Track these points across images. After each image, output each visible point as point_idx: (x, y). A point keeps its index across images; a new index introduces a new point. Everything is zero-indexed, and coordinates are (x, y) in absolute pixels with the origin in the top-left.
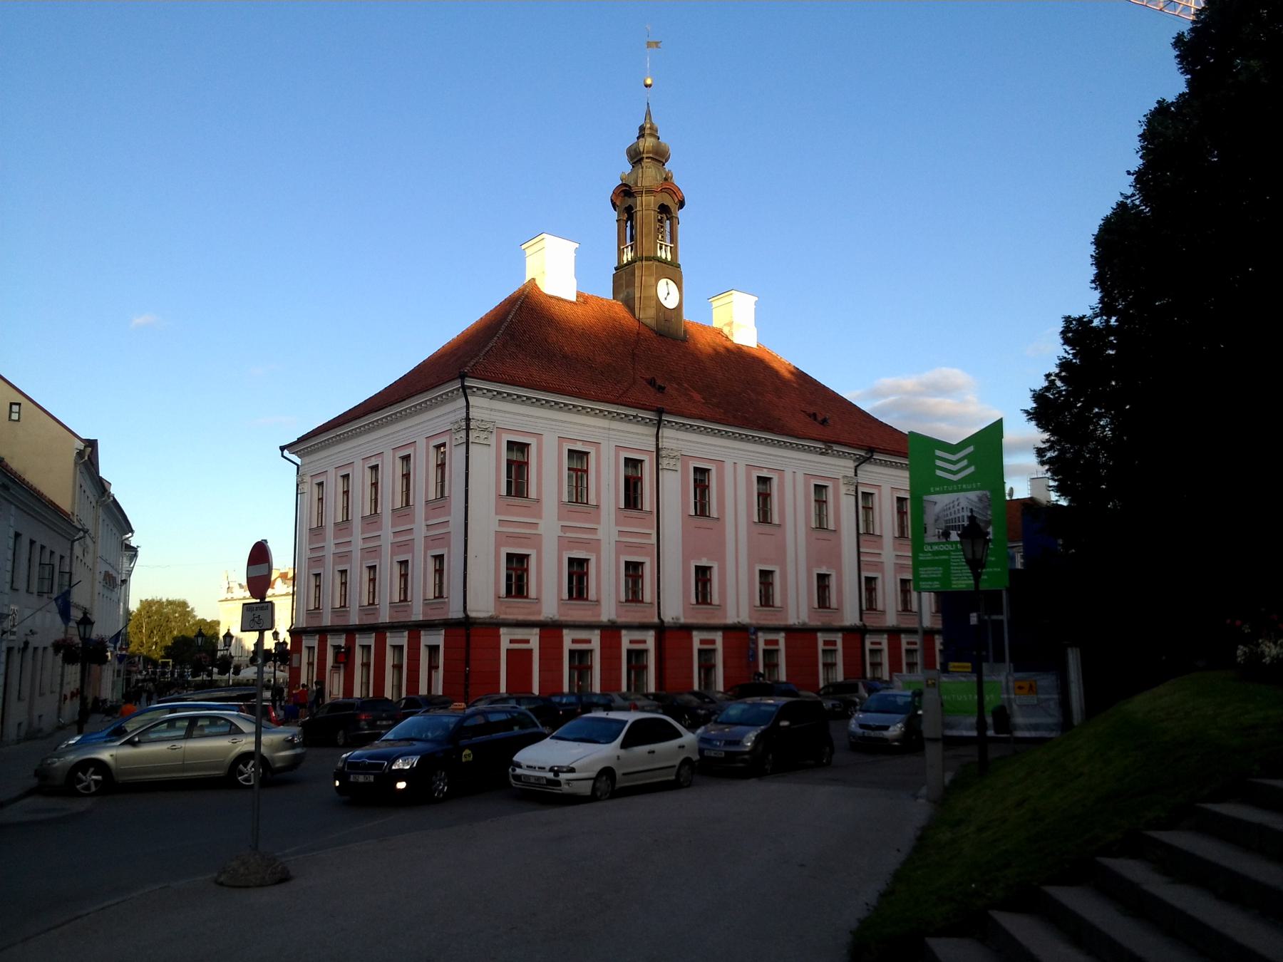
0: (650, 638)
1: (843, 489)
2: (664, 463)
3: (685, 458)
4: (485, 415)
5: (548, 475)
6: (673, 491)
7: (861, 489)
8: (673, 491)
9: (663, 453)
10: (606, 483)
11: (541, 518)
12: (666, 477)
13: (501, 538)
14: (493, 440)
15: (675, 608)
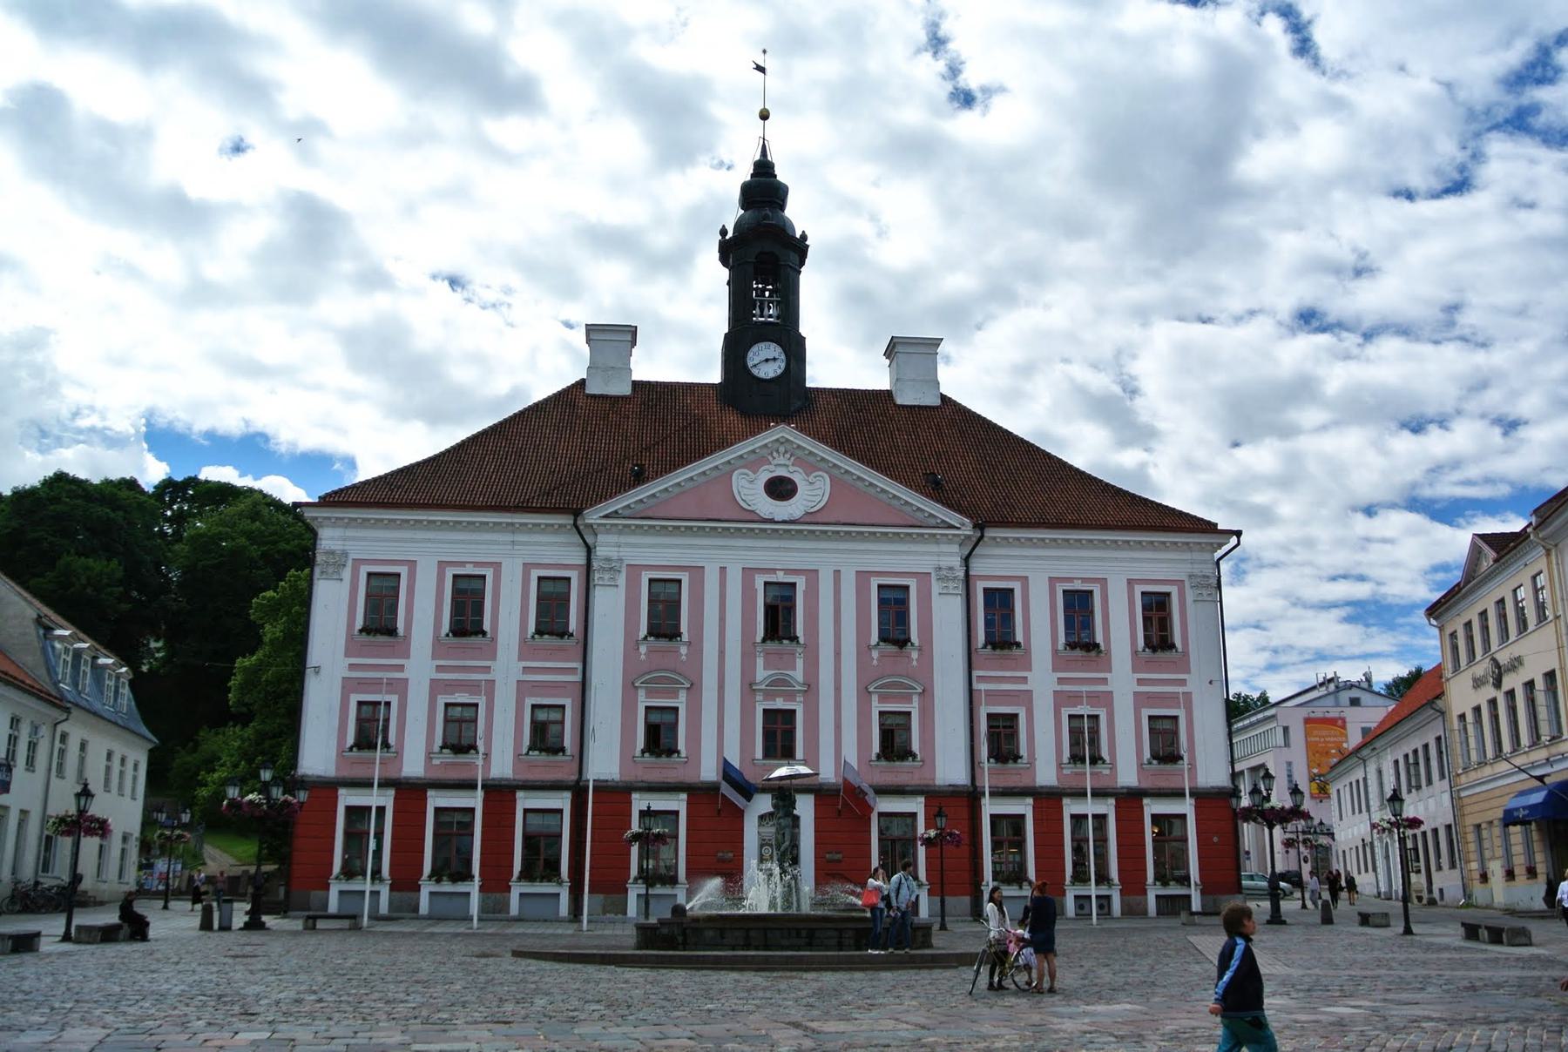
0: (563, 801)
1: (936, 588)
2: (597, 576)
3: (634, 570)
4: (336, 546)
5: (424, 612)
6: (612, 617)
7: (979, 588)
8: (612, 617)
9: (595, 565)
10: (510, 613)
11: (408, 657)
12: (600, 597)
13: (349, 686)
14: (347, 574)
15: (605, 760)
